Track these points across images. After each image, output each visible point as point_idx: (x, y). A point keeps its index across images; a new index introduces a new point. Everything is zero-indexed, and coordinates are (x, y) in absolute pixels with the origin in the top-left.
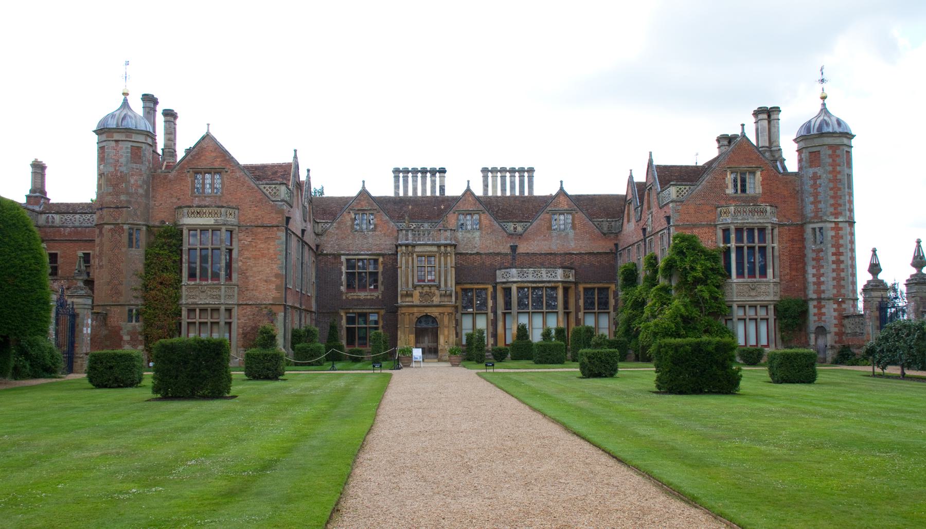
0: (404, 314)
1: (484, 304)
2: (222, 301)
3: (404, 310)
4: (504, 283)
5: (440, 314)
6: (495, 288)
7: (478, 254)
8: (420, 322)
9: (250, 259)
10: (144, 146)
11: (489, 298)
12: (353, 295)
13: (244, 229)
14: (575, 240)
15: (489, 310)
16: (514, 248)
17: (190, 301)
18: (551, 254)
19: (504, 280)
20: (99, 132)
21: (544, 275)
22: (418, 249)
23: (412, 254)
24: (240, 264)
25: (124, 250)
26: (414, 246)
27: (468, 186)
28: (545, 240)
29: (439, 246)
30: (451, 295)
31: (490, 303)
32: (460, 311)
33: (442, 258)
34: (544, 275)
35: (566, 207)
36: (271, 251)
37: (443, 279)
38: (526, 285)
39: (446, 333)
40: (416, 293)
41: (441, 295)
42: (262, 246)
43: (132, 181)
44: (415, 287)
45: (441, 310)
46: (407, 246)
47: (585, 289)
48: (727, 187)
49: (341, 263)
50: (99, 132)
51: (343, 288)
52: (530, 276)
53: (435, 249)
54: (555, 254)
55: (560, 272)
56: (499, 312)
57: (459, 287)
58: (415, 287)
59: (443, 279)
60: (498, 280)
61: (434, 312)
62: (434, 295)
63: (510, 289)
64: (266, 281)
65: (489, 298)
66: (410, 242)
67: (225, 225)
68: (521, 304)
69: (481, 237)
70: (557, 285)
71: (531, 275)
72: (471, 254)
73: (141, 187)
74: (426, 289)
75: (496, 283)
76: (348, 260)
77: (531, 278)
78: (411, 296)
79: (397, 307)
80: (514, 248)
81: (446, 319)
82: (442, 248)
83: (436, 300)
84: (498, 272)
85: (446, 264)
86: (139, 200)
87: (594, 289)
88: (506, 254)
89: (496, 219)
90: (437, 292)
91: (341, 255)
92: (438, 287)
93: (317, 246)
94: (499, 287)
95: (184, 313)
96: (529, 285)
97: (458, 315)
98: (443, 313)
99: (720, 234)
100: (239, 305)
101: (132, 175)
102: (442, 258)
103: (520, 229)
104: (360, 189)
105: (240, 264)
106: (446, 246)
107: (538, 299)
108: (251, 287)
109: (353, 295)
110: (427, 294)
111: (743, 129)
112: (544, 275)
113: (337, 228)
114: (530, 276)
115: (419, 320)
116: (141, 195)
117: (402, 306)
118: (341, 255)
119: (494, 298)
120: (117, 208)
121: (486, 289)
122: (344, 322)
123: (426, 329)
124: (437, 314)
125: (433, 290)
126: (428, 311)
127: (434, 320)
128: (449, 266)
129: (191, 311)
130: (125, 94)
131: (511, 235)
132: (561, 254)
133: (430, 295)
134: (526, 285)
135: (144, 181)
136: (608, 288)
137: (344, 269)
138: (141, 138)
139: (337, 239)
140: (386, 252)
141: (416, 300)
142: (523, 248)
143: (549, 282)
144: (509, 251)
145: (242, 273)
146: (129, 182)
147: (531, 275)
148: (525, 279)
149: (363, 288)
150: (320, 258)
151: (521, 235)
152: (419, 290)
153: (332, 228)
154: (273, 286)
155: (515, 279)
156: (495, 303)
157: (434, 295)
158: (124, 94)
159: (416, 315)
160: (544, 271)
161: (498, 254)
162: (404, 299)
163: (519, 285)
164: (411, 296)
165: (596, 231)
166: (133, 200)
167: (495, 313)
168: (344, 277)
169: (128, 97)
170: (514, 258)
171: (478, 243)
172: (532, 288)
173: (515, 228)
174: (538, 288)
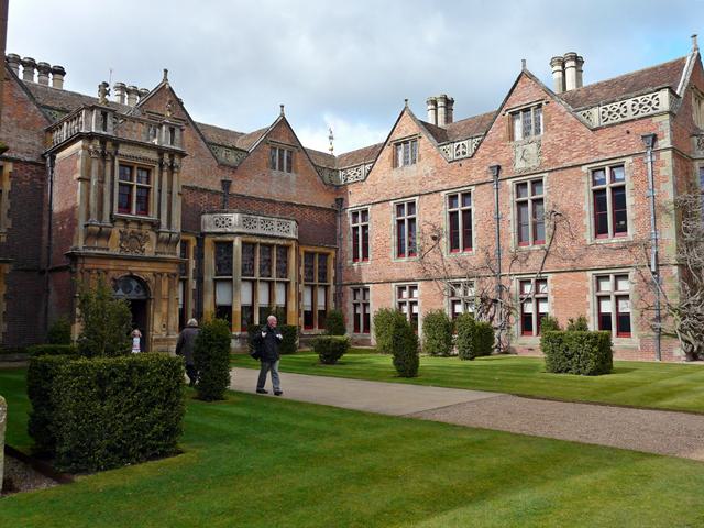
0: (89, 271)
3: (89, 264)
14: (297, 186)
16: (226, 184)
18: (270, 201)
22: (123, 150)
26: (117, 143)
27: (166, 79)
28: (263, 180)
29: (160, 151)
33: (165, 174)
39: (164, 309)
41: (159, 241)
44: (113, 220)
45: (157, 267)
46: (104, 139)
47: (306, 253)
52: (259, 226)
53: (154, 156)
54: (275, 202)
60: (207, 230)
61: (145, 271)
62: (147, 238)
63: (231, 242)
66: (110, 133)
68: (248, 269)
70: (290, 243)
74: (133, 227)
75: (204, 235)
78: (108, 236)
79: (74, 257)
80: (226, 184)
83: (150, 249)
87: (313, 254)
88: (217, 193)
90: (152, 235)
92: (155, 226)
94: (208, 240)
96: (258, 240)
102: (165, 174)
110: (134, 235)
114: (259, 226)
119: (200, 256)
124: (149, 276)
125: (146, 228)
126: (135, 267)
127: (143, 284)
131: (222, 165)
132: (280, 203)
133: (139, 238)
136: (328, 254)
140: (19, 156)
142: (238, 187)
143: (282, 238)
152: (120, 226)
157: (147, 238)
159: (112, 274)
161: (204, 191)
165: (318, 179)
167: (200, 279)
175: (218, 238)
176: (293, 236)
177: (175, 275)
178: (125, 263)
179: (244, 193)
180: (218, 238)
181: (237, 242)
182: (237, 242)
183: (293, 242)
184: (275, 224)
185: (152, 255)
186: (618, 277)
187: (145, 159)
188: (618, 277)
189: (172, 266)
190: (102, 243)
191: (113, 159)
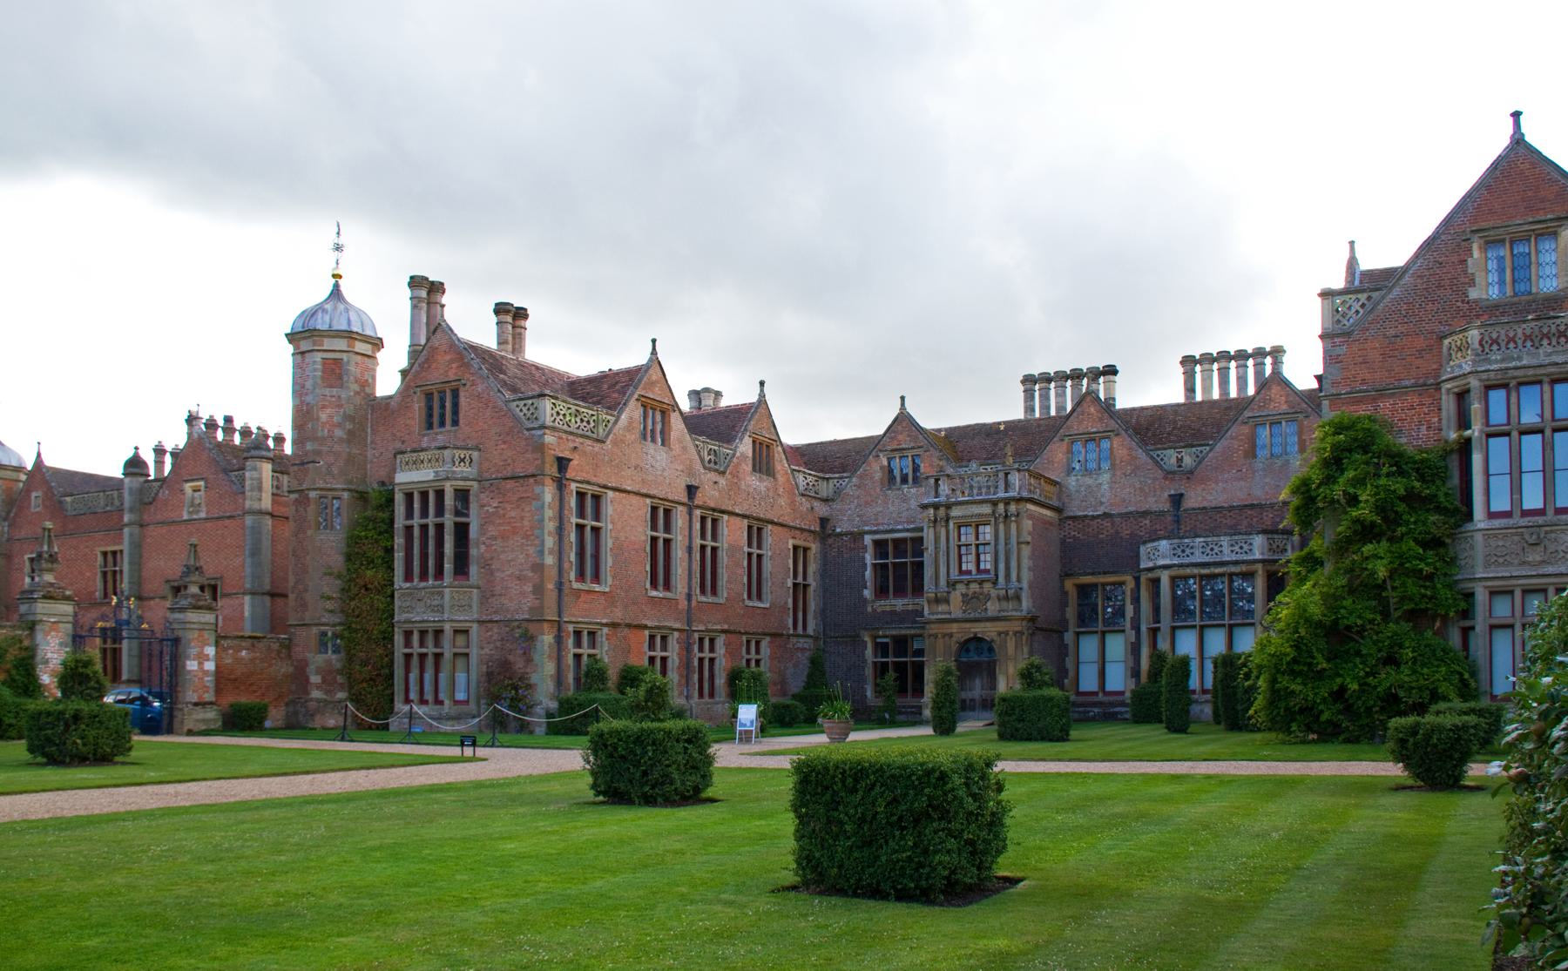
0: (936, 636)
1: (1120, 612)
2: (446, 616)
4: (1150, 570)
5: (999, 634)
6: (1137, 580)
7: (1106, 515)
8: (968, 651)
9: (495, 538)
10: (345, 356)
11: (1128, 601)
12: (885, 605)
13: (487, 484)
15: (1128, 625)
16: (1177, 500)
17: (405, 616)
18: (1252, 506)
19: (1151, 565)
20: (292, 337)
21: (1226, 550)
22: (955, 512)
23: (947, 521)
24: (483, 548)
25: (309, 532)
26: (948, 507)
29: (995, 503)
30: (1018, 598)
31: (1129, 610)
32: (1072, 628)
33: (1001, 527)
34: (1226, 550)
35: (1284, 407)
36: (526, 523)
37: (1002, 566)
38: (1188, 571)
40: (956, 597)
42: (513, 514)
43: (324, 416)
44: (952, 585)
45: (1001, 626)
46: (936, 506)
48: (1472, 283)
49: (865, 548)
50: (292, 337)
51: (867, 593)
53: (987, 509)
54: (1260, 506)
55: (1259, 541)
56: (1144, 628)
57: (1069, 584)
58: (952, 585)
59: (1002, 566)
61: (988, 630)
64: (519, 578)
65: (1128, 601)
67: (447, 479)
69: (1113, 482)
71: (1198, 551)
72: (1093, 518)
73: (339, 425)
76: (877, 543)
77: (1198, 558)
78: (947, 601)
80: (1177, 500)
81: (1011, 645)
82: (1001, 507)
83: (992, 608)
84: (1142, 549)
85: (1007, 539)
86: (337, 448)
88: (1161, 513)
89: (1144, 443)
90: (993, 593)
91: (862, 534)
93: (824, 521)
94: (1143, 579)
95: (399, 638)
96: (1196, 571)
97: (1069, 637)
98: (1007, 633)
99: (1448, 404)
100: (481, 622)
101: (324, 407)
102: (1001, 527)
103: (1188, 461)
104: (894, 412)
105: (483, 548)
106: (1007, 502)
107: (1214, 599)
108: (498, 589)
109: (885, 605)
110: (975, 596)
111: (1517, 125)
112: (1226, 549)
113: (859, 487)
114: (1197, 552)
115: (965, 646)
116: (341, 440)
117: (929, 622)
118: (862, 534)
119: (1136, 600)
120: (303, 464)
121: (1121, 584)
122: (869, 651)
123: (978, 664)
124: (993, 635)
125: (987, 586)
126: (978, 629)
128: (1014, 540)
129: (408, 635)
130: (337, 276)
131: (1169, 475)
134: (1188, 571)
135: (347, 417)
137: (869, 559)
138: (341, 344)
139: (859, 505)
141: (955, 608)
142: (1195, 498)
143: (1236, 563)
144: (1166, 507)
145: (486, 565)
146: (318, 419)
147: (1198, 551)
148: (1186, 561)
149: (900, 592)
150: (830, 541)
151: (1191, 472)
152: (961, 588)
153: (850, 485)
154: (528, 588)
155: (1168, 562)
156: (1137, 611)
158: (334, 276)
160: (1225, 541)
161: (1145, 514)
162: (934, 608)
163: (1175, 572)
164: (947, 601)
166: (325, 449)
168: (868, 573)
169: (341, 282)
170: (1177, 520)
171: (1108, 494)
172: (1202, 577)
173: (1180, 460)
174: (1215, 576)
175: (1150, 575)
176: (1258, 556)
177: (1022, 633)
178: (968, 625)
179: (1205, 504)
180: (1150, 575)
181: (1165, 578)
182: (1165, 578)
183: (1259, 567)
184: (1225, 544)
185: (996, 614)
186: (1527, 592)
187: (980, 515)
188: (1527, 592)
189: (1017, 623)
190: (942, 608)
191: (947, 526)
